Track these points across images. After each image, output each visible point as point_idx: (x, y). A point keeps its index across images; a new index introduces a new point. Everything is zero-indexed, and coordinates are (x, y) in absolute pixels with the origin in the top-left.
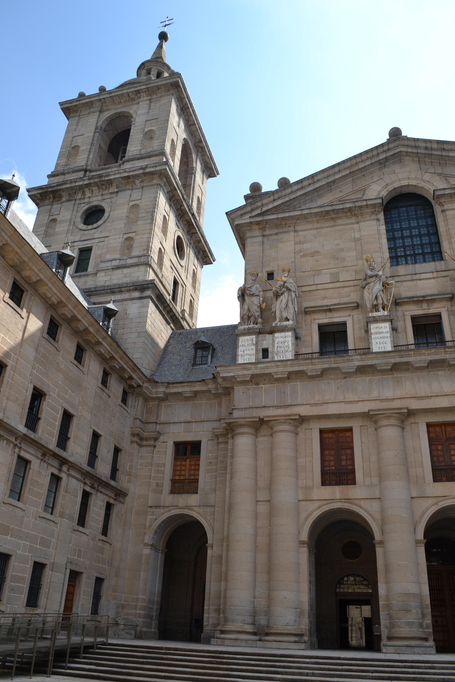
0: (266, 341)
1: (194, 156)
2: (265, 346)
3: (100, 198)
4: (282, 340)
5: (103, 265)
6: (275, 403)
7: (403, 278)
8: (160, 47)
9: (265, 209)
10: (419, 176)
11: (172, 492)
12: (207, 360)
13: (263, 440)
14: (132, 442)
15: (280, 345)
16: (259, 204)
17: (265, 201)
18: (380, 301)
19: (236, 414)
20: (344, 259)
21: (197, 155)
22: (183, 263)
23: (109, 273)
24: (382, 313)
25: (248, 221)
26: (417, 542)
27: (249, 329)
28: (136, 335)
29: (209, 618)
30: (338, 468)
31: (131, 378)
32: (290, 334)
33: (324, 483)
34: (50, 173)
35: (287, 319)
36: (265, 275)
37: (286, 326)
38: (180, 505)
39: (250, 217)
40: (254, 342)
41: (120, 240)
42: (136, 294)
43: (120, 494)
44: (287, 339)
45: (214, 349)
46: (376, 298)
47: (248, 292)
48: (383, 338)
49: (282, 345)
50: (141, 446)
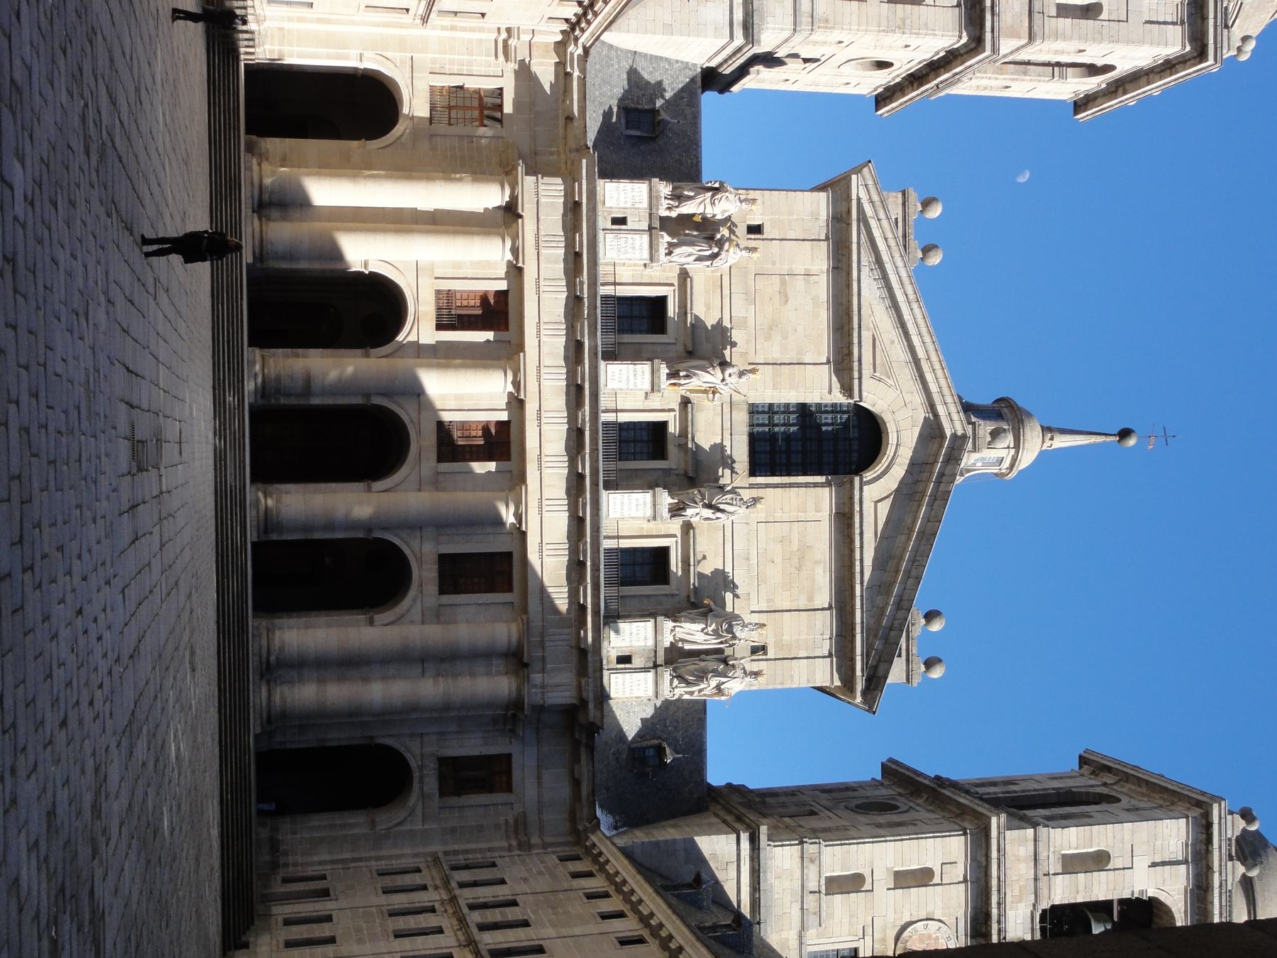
0: (638, 221)
2: (629, 220)
4: (637, 244)
6: (541, 233)
7: (727, 417)
9: (873, 223)
10: (898, 460)
12: (633, 128)
15: (630, 241)
16: (882, 215)
17: (885, 223)
18: (682, 382)
19: (530, 180)
20: (768, 338)
24: (664, 382)
25: (854, 197)
27: (658, 198)
29: (274, 145)
31: (583, 31)
32: (646, 254)
33: (438, 292)
35: (670, 253)
37: (657, 251)
38: (414, 102)
39: (859, 199)
40: (637, 206)
42: (739, 15)
43: (425, 19)
44: (637, 251)
45: (653, 139)
46: (687, 377)
47: (719, 196)
48: (628, 379)
49: (629, 244)
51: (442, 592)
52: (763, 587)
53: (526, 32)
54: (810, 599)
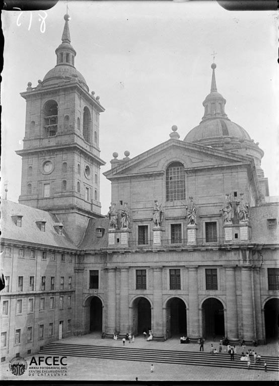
1: (91, 110)
3: (49, 157)
5: (55, 195)
8: (66, 27)
11: (90, 288)
13: (118, 273)
14: (75, 272)
18: (158, 222)
21: (92, 109)
22: (89, 177)
23: (59, 199)
26: (163, 309)
28: (72, 229)
30: (141, 283)
34: (23, 139)
35: (126, 226)
36: (119, 203)
41: (61, 182)
46: (157, 220)
50: (78, 273)
51: (217, 289)
52: (216, 195)
53: (75, 265)
54: (220, 180)
